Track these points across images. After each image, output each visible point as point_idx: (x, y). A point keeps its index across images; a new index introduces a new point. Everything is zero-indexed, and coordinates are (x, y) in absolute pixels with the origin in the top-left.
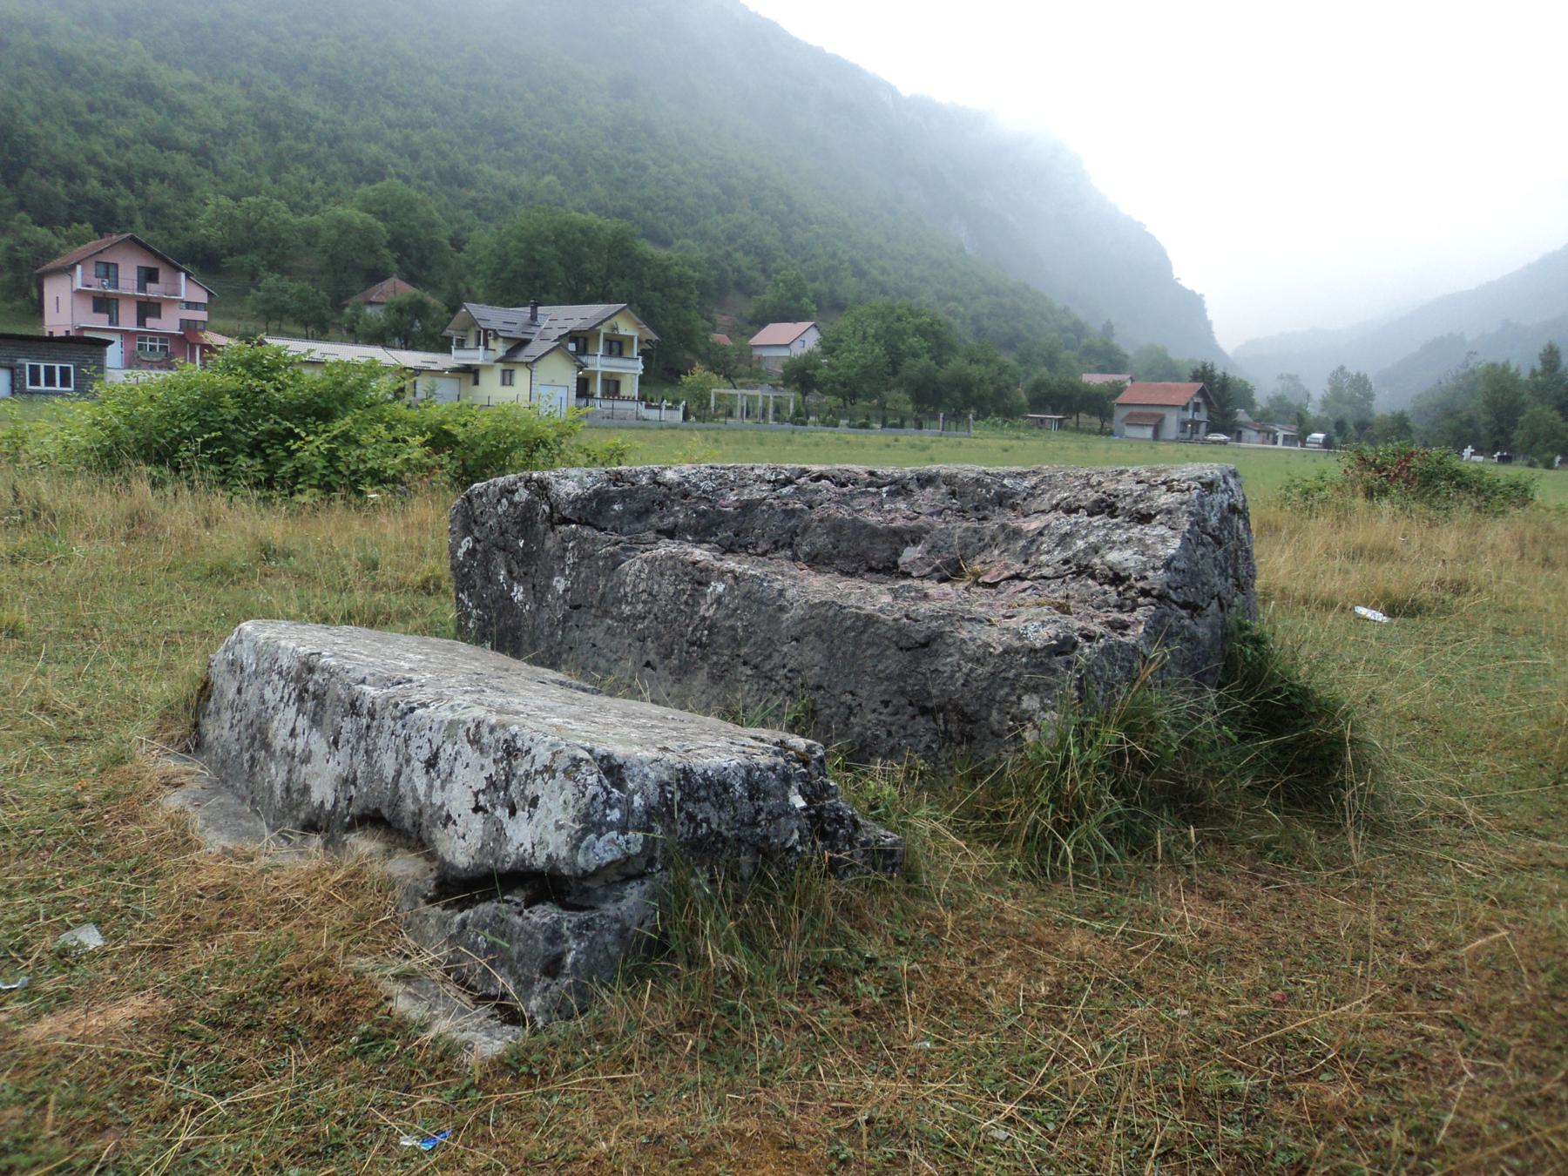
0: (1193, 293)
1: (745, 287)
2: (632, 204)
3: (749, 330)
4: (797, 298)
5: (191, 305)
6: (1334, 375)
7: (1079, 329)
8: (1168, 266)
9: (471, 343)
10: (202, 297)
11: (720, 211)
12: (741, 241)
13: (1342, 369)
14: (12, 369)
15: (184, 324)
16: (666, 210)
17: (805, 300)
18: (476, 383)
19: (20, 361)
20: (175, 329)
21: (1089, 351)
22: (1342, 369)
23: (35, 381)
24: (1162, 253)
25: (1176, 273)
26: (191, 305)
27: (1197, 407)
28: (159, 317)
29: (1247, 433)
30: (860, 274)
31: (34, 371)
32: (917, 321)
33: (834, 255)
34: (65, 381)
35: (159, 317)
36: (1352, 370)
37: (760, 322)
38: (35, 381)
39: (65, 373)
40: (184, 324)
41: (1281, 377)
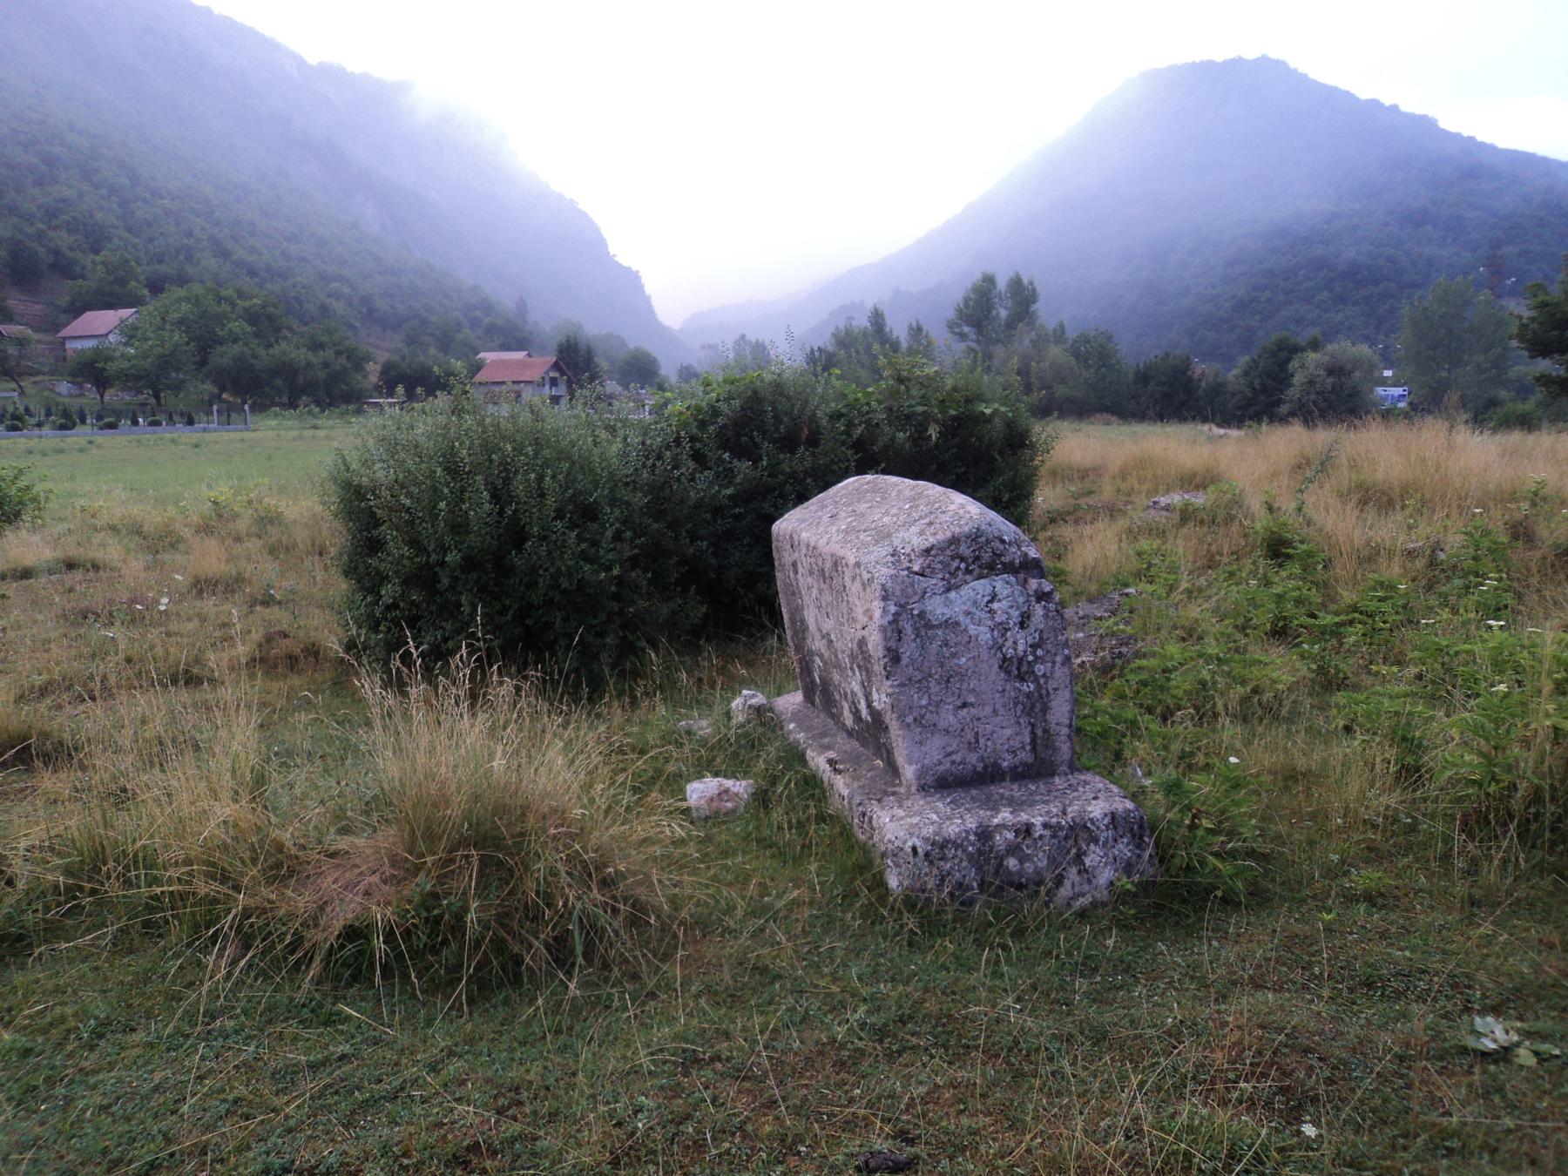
0: (629, 269)
1: (63, 268)
3: (63, 318)
4: (123, 282)
6: (737, 343)
7: (487, 307)
8: (601, 243)
11: (39, 183)
12: (66, 218)
13: (743, 337)
17: (133, 283)
21: (492, 330)
22: (743, 337)
24: (596, 231)
25: (612, 250)
27: (554, 382)
30: (225, 254)
32: (247, 304)
33: (189, 234)
36: (752, 337)
37: (76, 310)
41: (703, 347)
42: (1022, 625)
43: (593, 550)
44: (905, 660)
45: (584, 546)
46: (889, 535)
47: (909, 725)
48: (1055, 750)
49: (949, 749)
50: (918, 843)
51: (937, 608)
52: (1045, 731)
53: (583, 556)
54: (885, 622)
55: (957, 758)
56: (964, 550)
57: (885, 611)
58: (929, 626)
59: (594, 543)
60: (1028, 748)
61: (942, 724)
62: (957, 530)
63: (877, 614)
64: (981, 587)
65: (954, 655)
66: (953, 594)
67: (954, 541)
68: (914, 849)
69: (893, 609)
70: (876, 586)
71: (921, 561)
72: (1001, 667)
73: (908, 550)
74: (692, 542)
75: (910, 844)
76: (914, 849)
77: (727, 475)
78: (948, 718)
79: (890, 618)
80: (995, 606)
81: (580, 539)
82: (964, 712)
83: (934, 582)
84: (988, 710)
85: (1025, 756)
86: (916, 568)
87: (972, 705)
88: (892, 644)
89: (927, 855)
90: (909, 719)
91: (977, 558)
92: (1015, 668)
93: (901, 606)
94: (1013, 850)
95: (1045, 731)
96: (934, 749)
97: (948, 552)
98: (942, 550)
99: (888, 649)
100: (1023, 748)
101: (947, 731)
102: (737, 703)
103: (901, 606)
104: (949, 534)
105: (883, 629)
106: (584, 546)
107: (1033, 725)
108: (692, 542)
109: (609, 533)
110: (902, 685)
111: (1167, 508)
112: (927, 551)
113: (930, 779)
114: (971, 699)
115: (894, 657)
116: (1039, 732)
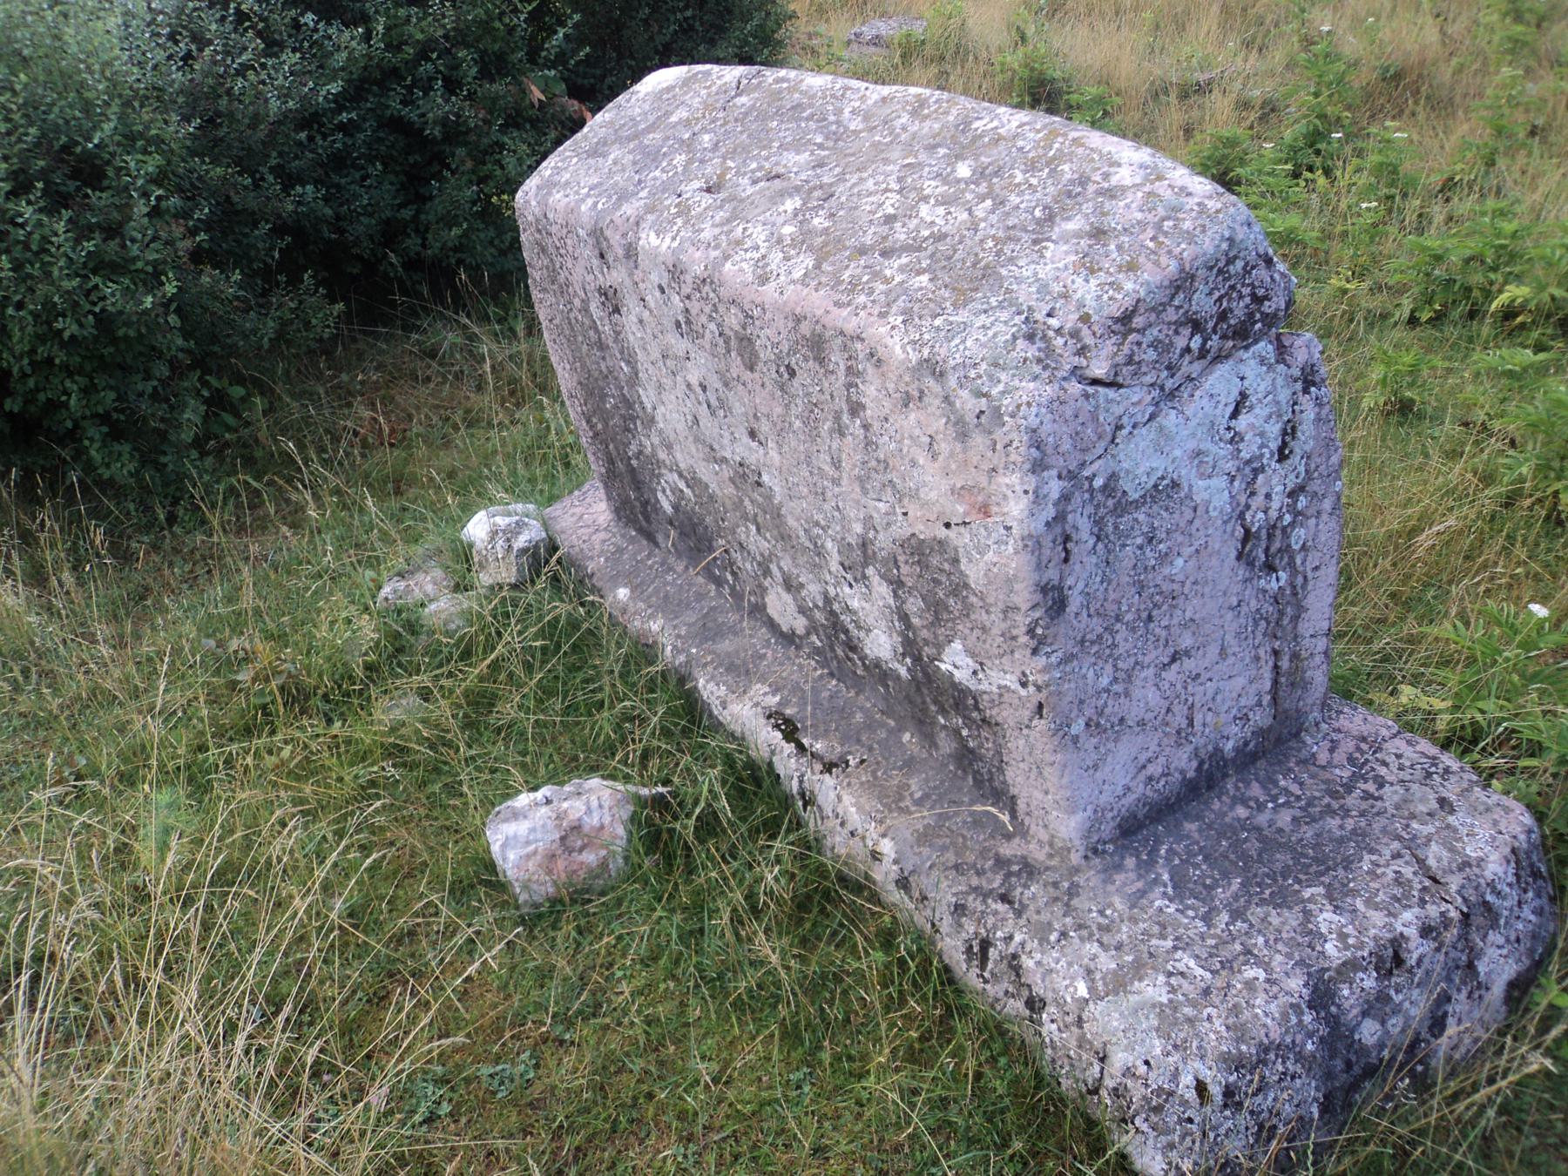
42: (1282, 456)
43: (113, 245)
44: (1075, 602)
45: (90, 246)
46: (986, 275)
47: (1075, 740)
48: (1305, 685)
49: (1143, 758)
50: (1207, 1075)
51: (1140, 462)
52: (1295, 656)
53: (100, 265)
54: (1038, 526)
55: (1155, 769)
56: (1203, 303)
57: (1038, 498)
58: (1123, 507)
59: (112, 231)
60: (1267, 699)
61: (1134, 712)
62: (1188, 251)
63: (1016, 509)
64: (1221, 382)
65: (1164, 558)
66: (1170, 419)
67: (1183, 283)
68: (1201, 1088)
69: (1055, 488)
70: (1012, 432)
71: (1109, 346)
72: (1239, 558)
73: (1071, 320)
74: (287, 188)
75: (1187, 1080)
76: (1201, 1088)
77: (317, 56)
78: (1146, 696)
79: (1050, 512)
80: (1242, 423)
81: (81, 232)
82: (1171, 674)
83: (1136, 397)
84: (1213, 651)
85: (1261, 718)
86: (1099, 370)
87: (1187, 653)
88: (1052, 574)
89: (1229, 1092)
90: (1078, 727)
91: (1223, 316)
92: (1262, 549)
93: (1072, 476)
94: (1377, 1006)
95: (1295, 656)
96: (1123, 775)
97: (1171, 315)
98: (1158, 309)
99: (1044, 589)
100: (1259, 704)
101: (1142, 723)
102: (478, 528)
103: (1072, 476)
104: (1173, 266)
105: (1032, 544)
106: (90, 246)
107: (1276, 653)
108: (287, 188)
109: (141, 208)
110: (1067, 659)
111: (876, 41)
112: (1126, 318)
113: (1107, 829)
114: (1187, 641)
115: (1054, 600)
116: (1285, 664)
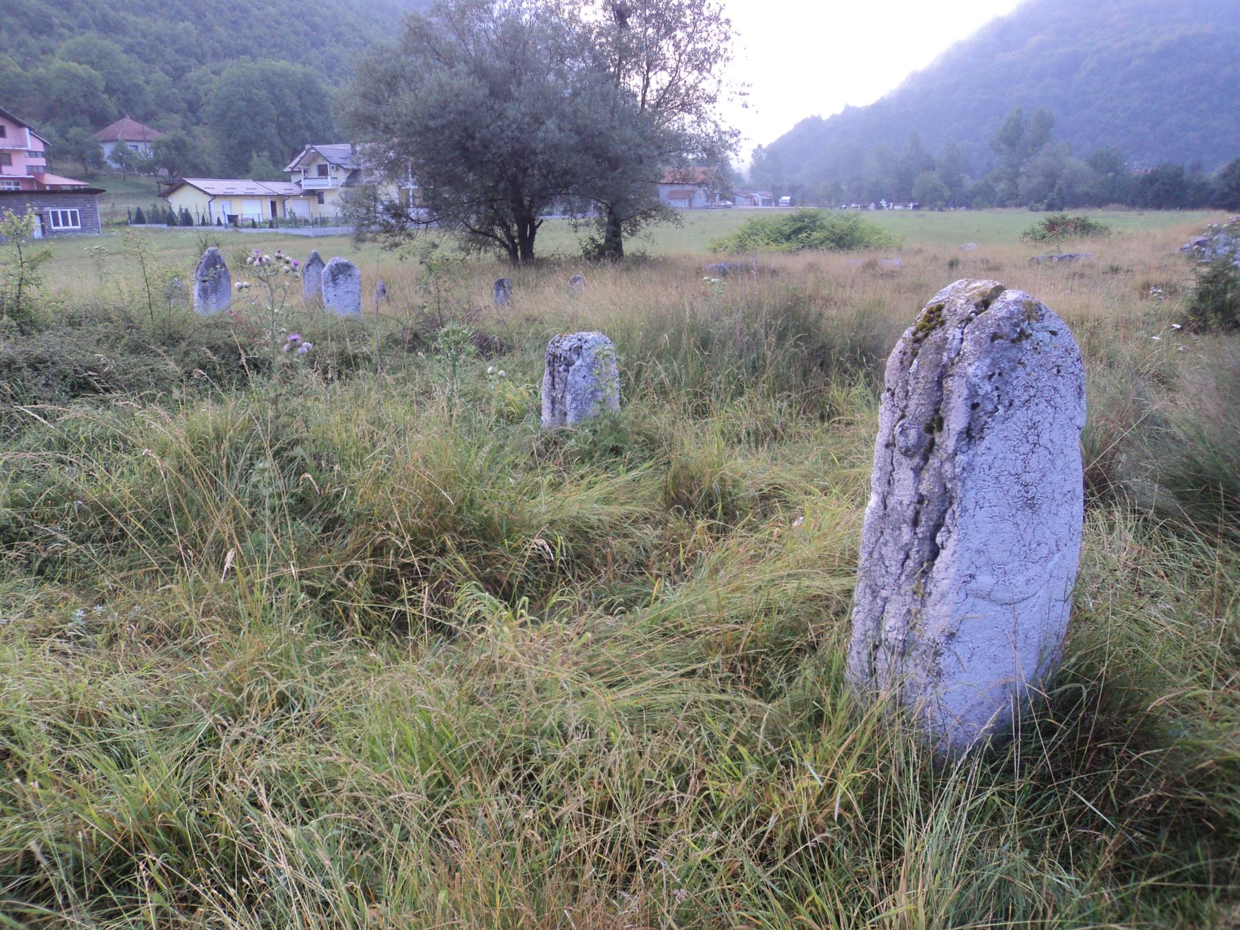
2: (250, 43)
5: (33, 154)
9: (314, 172)
10: (40, 147)
14: (41, 216)
15: (31, 169)
16: (275, 46)
18: (321, 201)
19: (46, 209)
20: (23, 174)
23: (56, 224)
26: (33, 154)
28: (10, 164)
29: (738, 199)
31: (55, 214)
34: (75, 223)
35: (10, 164)
38: (56, 224)
39: (73, 214)
40: (31, 169)
